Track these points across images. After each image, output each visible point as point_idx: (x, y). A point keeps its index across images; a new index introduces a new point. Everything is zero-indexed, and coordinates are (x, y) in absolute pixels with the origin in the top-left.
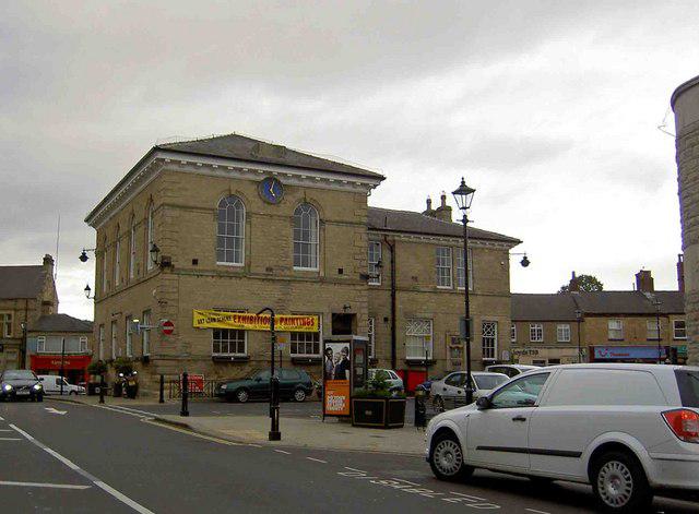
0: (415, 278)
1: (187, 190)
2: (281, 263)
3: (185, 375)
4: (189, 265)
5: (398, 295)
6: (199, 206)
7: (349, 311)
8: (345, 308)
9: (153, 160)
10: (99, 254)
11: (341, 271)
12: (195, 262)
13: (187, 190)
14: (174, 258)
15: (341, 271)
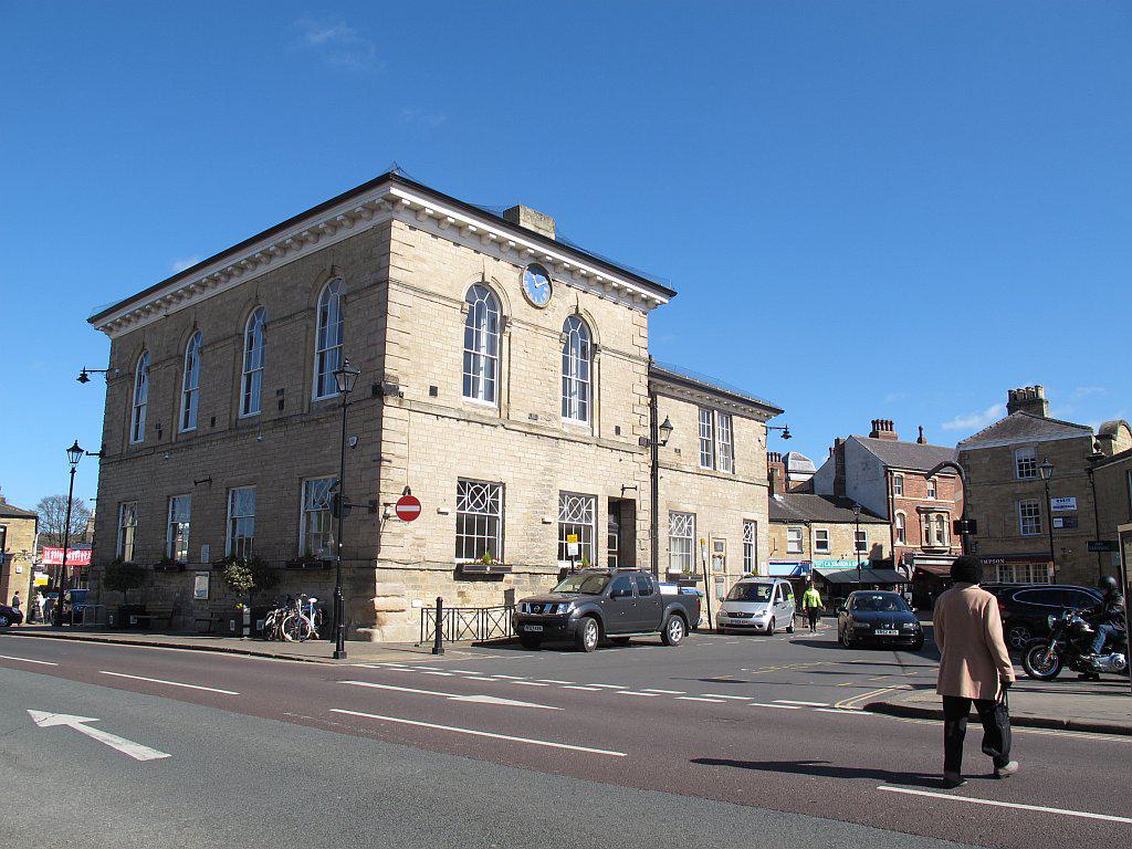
0: (678, 451)
1: (423, 260)
2: (548, 409)
3: (439, 601)
4: (425, 397)
5: (661, 472)
6: (440, 292)
7: (629, 495)
8: (623, 489)
9: (375, 196)
10: (111, 377)
11: (618, 430)
12: (433, 391)
13: (423, 260)
14: (402, 381)
15: (618, 430)
